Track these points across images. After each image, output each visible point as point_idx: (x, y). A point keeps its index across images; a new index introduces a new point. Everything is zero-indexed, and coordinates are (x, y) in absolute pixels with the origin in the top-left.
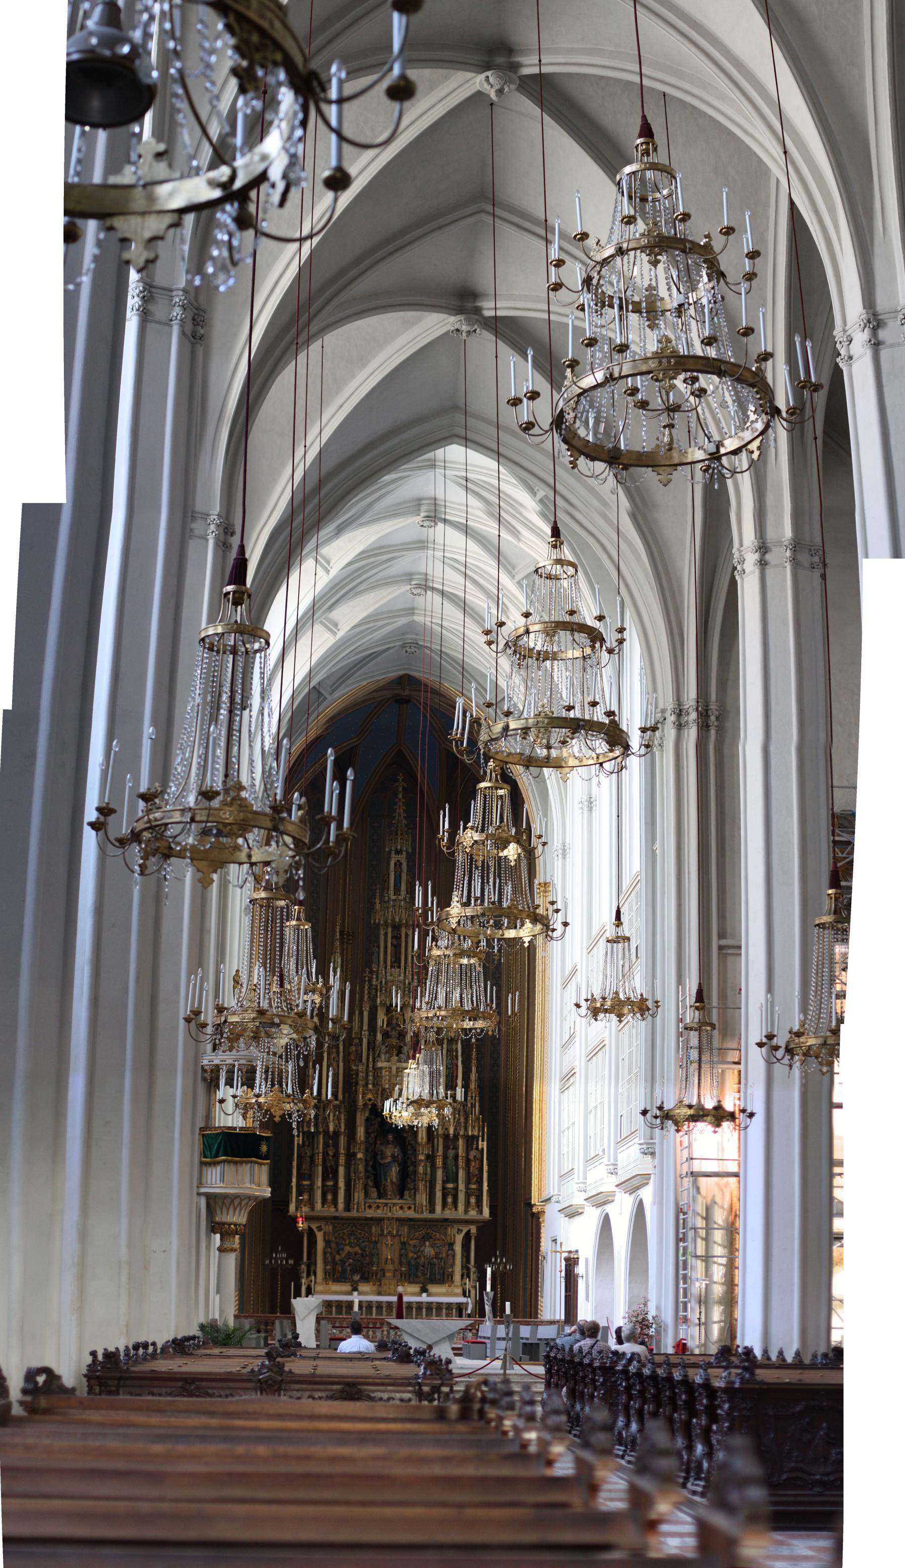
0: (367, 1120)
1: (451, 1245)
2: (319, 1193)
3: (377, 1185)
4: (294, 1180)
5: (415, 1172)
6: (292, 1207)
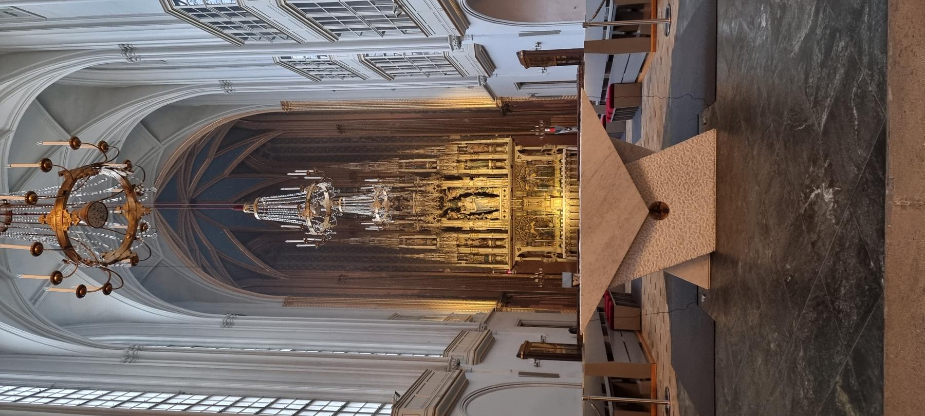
0: (449, 219)
1: (528, 162)
2: (496, 251)
3: (490, 212)
5: (482, 188)
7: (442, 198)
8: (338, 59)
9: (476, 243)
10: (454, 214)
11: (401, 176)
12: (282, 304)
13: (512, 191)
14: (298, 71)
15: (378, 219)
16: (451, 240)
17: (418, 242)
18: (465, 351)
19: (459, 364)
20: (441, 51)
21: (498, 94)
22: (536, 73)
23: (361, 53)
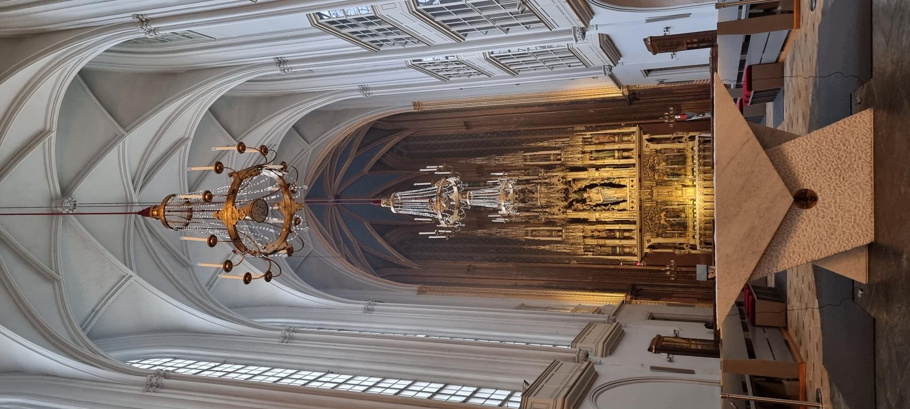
0: (575, 210)
1: (657, 151)
3: (617, 203)
4: (616, 257)
5: (608, 179)
6: (635, 259)
7: (567, 190)
8: (464, 59)
9: (603, 234)
10: (579, 206)
11: (526, 169)
12: (416, 293)
13: (640, 180)
14: (428, 72)
15: (504, 211)
16: (577, 231)
17: (543, 234)
18: (594, 342)
19: (587, 356)
20: (564, 43)
21: (624, 83)
22: (664, 59)
23: (487, 51)
